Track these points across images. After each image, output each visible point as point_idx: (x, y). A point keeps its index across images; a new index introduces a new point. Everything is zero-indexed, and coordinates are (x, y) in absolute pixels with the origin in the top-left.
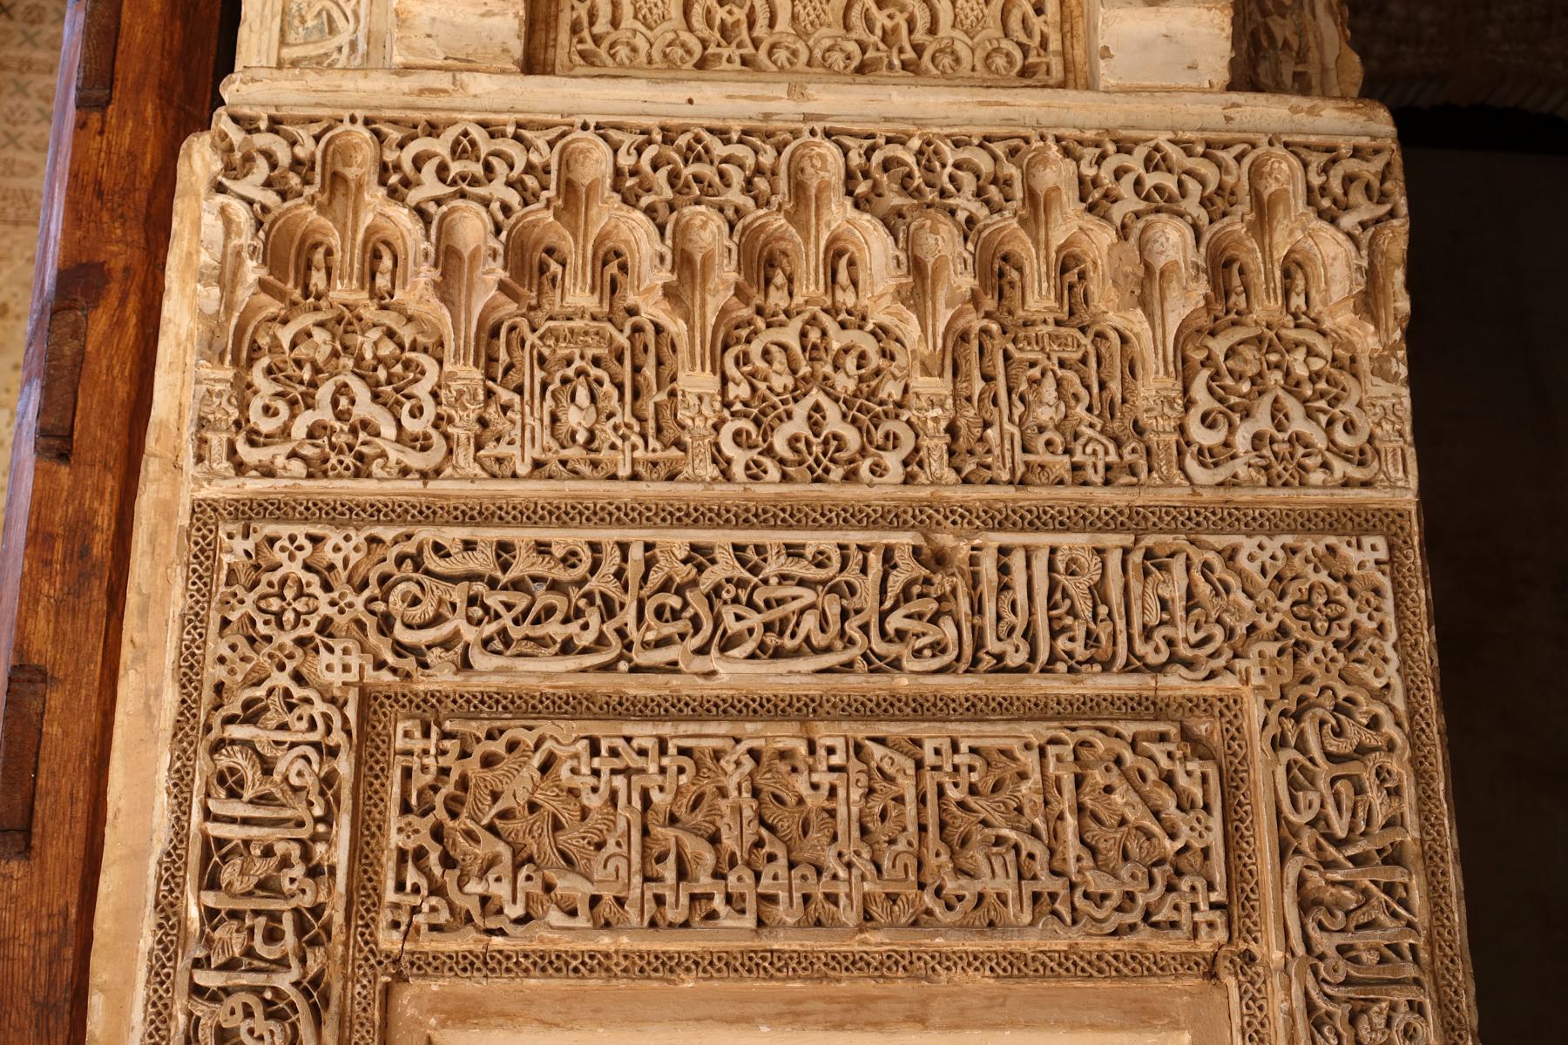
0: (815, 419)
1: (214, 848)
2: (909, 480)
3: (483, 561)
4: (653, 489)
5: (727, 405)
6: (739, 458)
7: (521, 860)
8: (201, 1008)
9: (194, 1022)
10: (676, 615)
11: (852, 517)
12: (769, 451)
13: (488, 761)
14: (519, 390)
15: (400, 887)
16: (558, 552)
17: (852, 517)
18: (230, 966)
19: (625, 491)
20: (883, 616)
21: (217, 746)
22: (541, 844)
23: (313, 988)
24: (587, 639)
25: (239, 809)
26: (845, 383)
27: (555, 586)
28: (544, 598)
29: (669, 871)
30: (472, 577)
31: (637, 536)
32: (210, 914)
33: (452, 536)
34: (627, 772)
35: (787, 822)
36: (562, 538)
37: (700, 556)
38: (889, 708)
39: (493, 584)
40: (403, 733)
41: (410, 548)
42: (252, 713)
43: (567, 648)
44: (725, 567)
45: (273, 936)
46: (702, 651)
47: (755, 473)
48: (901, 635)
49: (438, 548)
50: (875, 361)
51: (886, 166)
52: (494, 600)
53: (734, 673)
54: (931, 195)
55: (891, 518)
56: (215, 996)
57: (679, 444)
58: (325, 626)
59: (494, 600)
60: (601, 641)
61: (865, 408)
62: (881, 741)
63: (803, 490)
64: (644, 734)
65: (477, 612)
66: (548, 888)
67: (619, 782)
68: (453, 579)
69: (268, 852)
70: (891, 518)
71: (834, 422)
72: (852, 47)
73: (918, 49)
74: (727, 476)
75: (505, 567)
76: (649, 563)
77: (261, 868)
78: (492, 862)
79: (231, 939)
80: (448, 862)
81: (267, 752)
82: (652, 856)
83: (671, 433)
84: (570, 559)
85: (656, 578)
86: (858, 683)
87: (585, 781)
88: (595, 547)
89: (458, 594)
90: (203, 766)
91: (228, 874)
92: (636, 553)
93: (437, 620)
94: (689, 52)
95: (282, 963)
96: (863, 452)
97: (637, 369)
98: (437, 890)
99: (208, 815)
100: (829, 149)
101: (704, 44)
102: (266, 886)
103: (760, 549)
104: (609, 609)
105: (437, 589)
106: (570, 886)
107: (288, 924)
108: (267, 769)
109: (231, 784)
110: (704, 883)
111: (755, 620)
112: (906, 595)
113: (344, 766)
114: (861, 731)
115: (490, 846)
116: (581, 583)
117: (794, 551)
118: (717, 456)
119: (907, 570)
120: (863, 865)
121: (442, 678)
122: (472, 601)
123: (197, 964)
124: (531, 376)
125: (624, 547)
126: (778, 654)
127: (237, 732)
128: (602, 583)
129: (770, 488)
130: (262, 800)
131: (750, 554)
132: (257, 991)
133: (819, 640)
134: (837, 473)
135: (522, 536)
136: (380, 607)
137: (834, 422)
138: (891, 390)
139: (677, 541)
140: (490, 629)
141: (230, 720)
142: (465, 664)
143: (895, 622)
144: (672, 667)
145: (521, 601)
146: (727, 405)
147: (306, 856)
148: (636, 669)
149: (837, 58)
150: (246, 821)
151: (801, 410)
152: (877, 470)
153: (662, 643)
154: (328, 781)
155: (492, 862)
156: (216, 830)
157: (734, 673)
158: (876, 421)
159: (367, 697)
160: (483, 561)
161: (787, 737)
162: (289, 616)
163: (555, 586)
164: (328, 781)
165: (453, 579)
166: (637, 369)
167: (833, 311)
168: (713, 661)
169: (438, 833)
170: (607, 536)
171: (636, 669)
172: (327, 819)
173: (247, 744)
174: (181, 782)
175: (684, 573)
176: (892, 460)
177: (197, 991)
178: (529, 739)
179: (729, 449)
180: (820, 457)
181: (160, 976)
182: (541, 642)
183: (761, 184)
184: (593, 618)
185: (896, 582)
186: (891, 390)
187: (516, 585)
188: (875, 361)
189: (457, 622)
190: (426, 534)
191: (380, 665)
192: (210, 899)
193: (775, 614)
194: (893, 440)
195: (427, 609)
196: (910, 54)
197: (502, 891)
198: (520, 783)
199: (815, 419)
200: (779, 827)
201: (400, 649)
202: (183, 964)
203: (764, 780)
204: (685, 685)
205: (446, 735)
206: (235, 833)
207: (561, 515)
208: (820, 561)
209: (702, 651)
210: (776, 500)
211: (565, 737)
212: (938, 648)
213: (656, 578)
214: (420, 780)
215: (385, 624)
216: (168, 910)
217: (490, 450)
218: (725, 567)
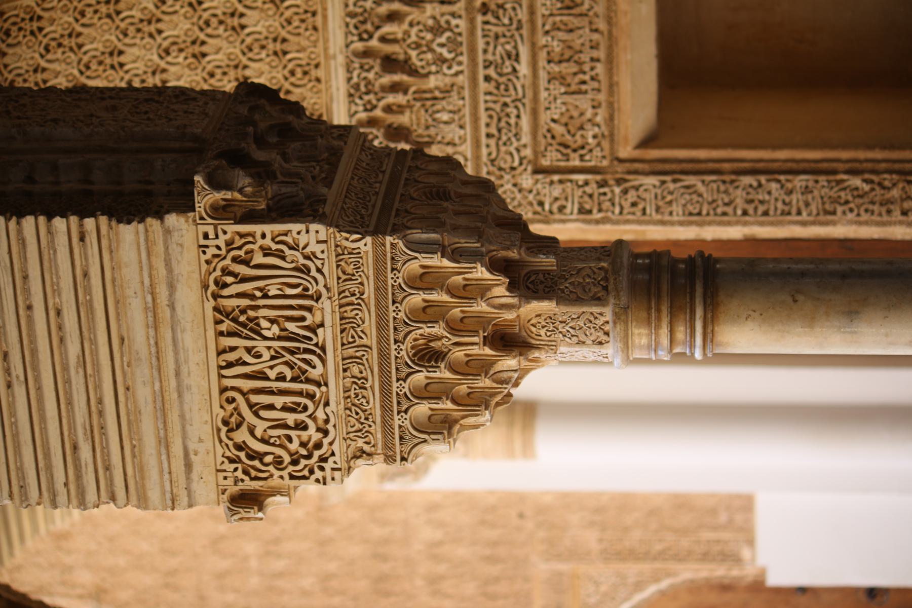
0: (442, 45)
1: (582, 211)
2: (460, 17)
3: (492, 142)
4: (466, 93)
5: (438, 72)
6: (455, 68)
7: (581, 128)
8: (625, 211)
9: (629, 213)
10: (507, 86)
11: (472, 31)
12: (453, 59)
13: (553, 137)
14: (437, 135)
15: (590, 161)
16: (488, 120)
17: (472, 31)
18: (613, 204)
19: (467, 101)
20: (504, 25)
21: (551, 212)
22: (577, 122)
23: (619, 182)
24: (515, 112)
25: (569, 205)
26: (429, 36)
27: (499, 120)
28: (503, 124)
29: (584, 87)
30: (497, 145)
31: (482, 98)
32: (600, 210)
33: (484, 151)
34: (555, 99)
35: (568, 53)
36: (484, 118)
37: (487, 79)
38: (532, 22)
39: (499, 139)
40: (545, 162)
41: (489, 163)
42: (541, 204)
43: (518, 116)
44: (491, 72)
45: (605, 194)
46: (517, 78)
47: (460, 63)
48: (511, 19)
49: (490, 154)
50: (421, 27)
51: (356, 27)
52: (504, 138)
53: (524, 69)
54: (366, 15)
55: (472, 21)
56: (622, 208)
57: (452, 85)
58: (515, 185)
59: (504, 138)
60: (516, 107)
61: (437, 30)
62: (544, 25)
63: (464, 49)
64: (543, 95)
65: (508, 143)
66: (589, 120)
67: (559, 101)
68: (498, 150)
69: (581, 197)
70: (472, 21)
71: (443, 40)
72: (308, 33)
73: (306, 12)
74: (461, 72)
75: (493, 136)
76: (490, 93)
77: (586, 198)
78: (582, 136)
79: (606, 205)
80: (583, 147)
81: (552, 199)
82: (579, 92)
83: (448, 88)
84: (491, 117)
85: (495, 91)
86: (525, 32)
87: (558, 111)
88: (487, 109)
89: (503, 149)
90: (558, 216)
91: (587, 207)
92: (488, 98)
93: (511, 154)
94: (314, 86)
95: (612, 191)
96: (451, 31)
97: (427, 99)
98: (591, 151)
99: (572, 213)
100: (353, 46)
101: (310, 81)
102: (591, 196)
103: (485, 61)
104: (505, 105)
105: (502, 155)
106: (589, 114)
107: (602, 190)
108: (556, 199)
109: (561, 209)
110: (587, 78)
111: (507, 63)
112: (498, 18)
113: (556, 178)
114: (540, 32)
115: (578, 137)
116: (498, 114)
117: (485, 51)
118: (457, 74)
119: (489, 17)
120: (581, 32)
121: (528, 152)
122: (505, 144)
123: (613, 212)
124: (432, 131)
125: (486, 102)
126: (517, 55)
127: (547, 207)
128: (498, 107)
129: (464, 58)
130: (566, 199)
131: (487, 63)
132: (620, 197)
133: (513, 44)
134: (459, 39)
135: (483, 130)
136: (508, 170)
137: (443, 40)
138: (430, 22)
139: (483, 86)
140: (513, 139)
141: (543, 209)
142: (525, 146)
143: (506, 21)
144: (523, 87)
145: (504, 131)
146: (438, 72)
147: (582, 186)
148: (524, 96)
149: (313, 38)
150: (573, 203)
151: (439, 50)
152: (457, 26)
153: (515, 89)
154: (561, 182)
155: (582, 136)
156: (576, 211)
157: (524, 69)
158: (440, 26)
159: (536, 171)
160: (492, 142)
161: (543, 55)
162: (512, 196)
163: (499, 120)
164: (561, 182)
165: (498, 150)
166: (427, 99)
167: (404, 40)
168: (521, 74)
169: (575, 151)
170: (482, 106)
171: (524, 96)
172: (571, 181)
173: (551, 205)
174: (563, 221)
175: (493, 84)
176: (454, 22)
177: (621, 213)
178: (546, 127)
179: (453, 71)
180: (454, 44)
181: (617, 222)
182: (517, 124)
183: (366, 67)
184: (508, 110)
185: (493, 20)
186: (430, 22)
187: (499, 130)
188: (421, 27)
189: (512, 149)
190: (484, 159)
191: (525, 170)
192: (595, 211)
193: (505, 57)
194: (448, 22)
195: (508, 158)
196: (309, 15)
197: (590, 134)
198: (559, 129)
199: (442, 45)
200: (569, 55)
201: (521, 164)
202: (613, 217)
203: (557, 59)
204: (528, 82)
205: (546, 150)
206: (576, 207)
207: (475, 119)
208: (488, 43)
209: (517, 78)
210: (469, 56)
211: (545, 117)
212: (514, 9)
213: (495, 91)
214: (559, 156)
215: (513, 169)
216: (597, 222)
217: (457, 141)
218: (491, 72)
